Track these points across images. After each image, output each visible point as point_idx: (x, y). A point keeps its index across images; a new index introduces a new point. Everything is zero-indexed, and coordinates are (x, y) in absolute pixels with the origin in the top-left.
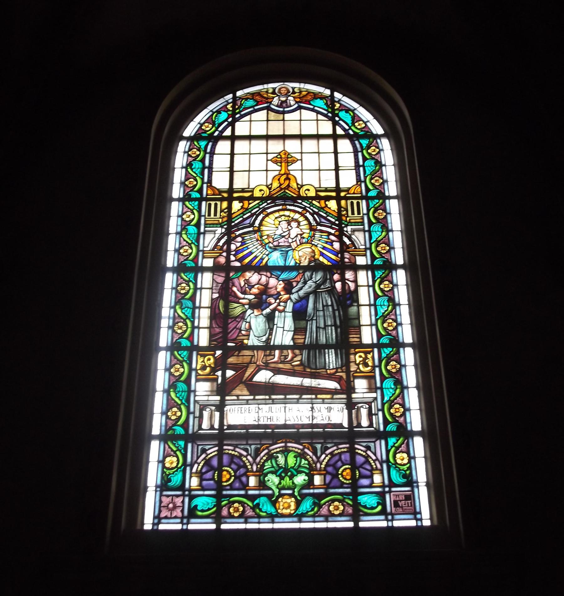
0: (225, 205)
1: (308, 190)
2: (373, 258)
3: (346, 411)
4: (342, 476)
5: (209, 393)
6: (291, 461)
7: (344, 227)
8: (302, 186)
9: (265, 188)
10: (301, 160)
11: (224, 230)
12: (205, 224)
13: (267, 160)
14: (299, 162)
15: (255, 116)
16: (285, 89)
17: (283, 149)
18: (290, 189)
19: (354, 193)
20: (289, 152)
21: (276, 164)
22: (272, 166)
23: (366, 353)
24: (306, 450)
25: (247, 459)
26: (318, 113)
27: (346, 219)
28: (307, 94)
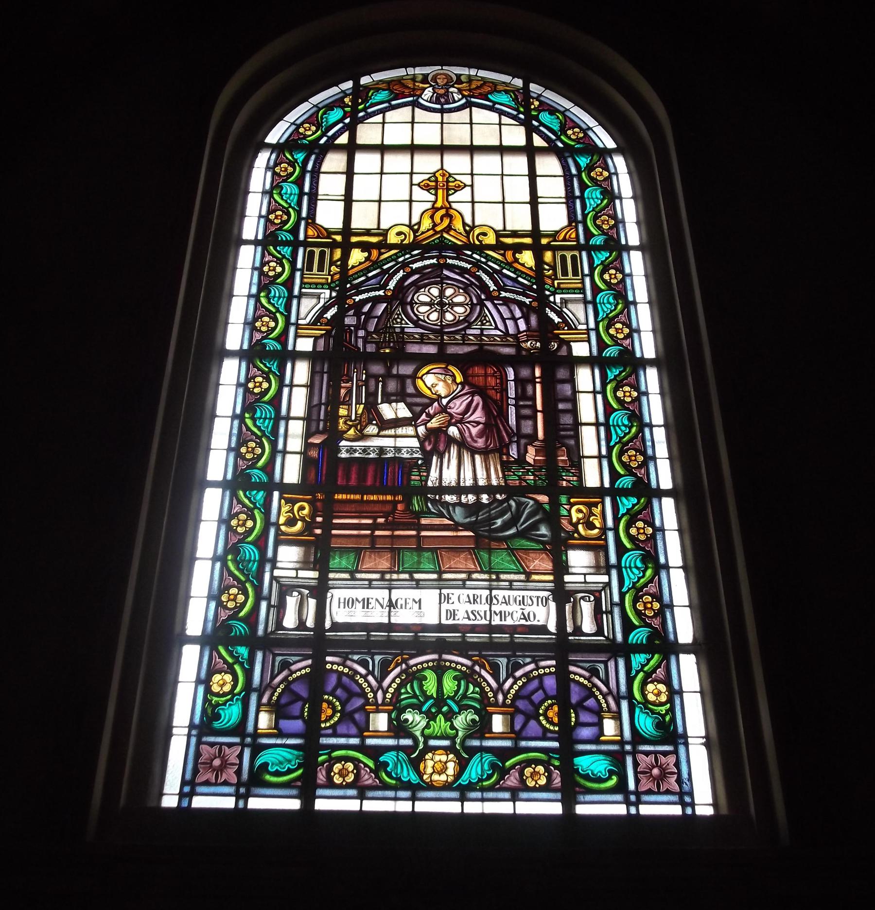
1: (485, 234)
2: (602, 345)
3: (553, 605)
5: (298, 566)
6: (449, 685)
7: (550, 295)
8: (473, 227)
9: (406, 230)
10: (472, 186)
11: (334, 294)
13: (412, 185)
14: (468, 189)
15: (390, 116)
16: (444, 77)
21: (428, 191)
22: (419, 194)
25: (366, 681)
26: (501, 113)
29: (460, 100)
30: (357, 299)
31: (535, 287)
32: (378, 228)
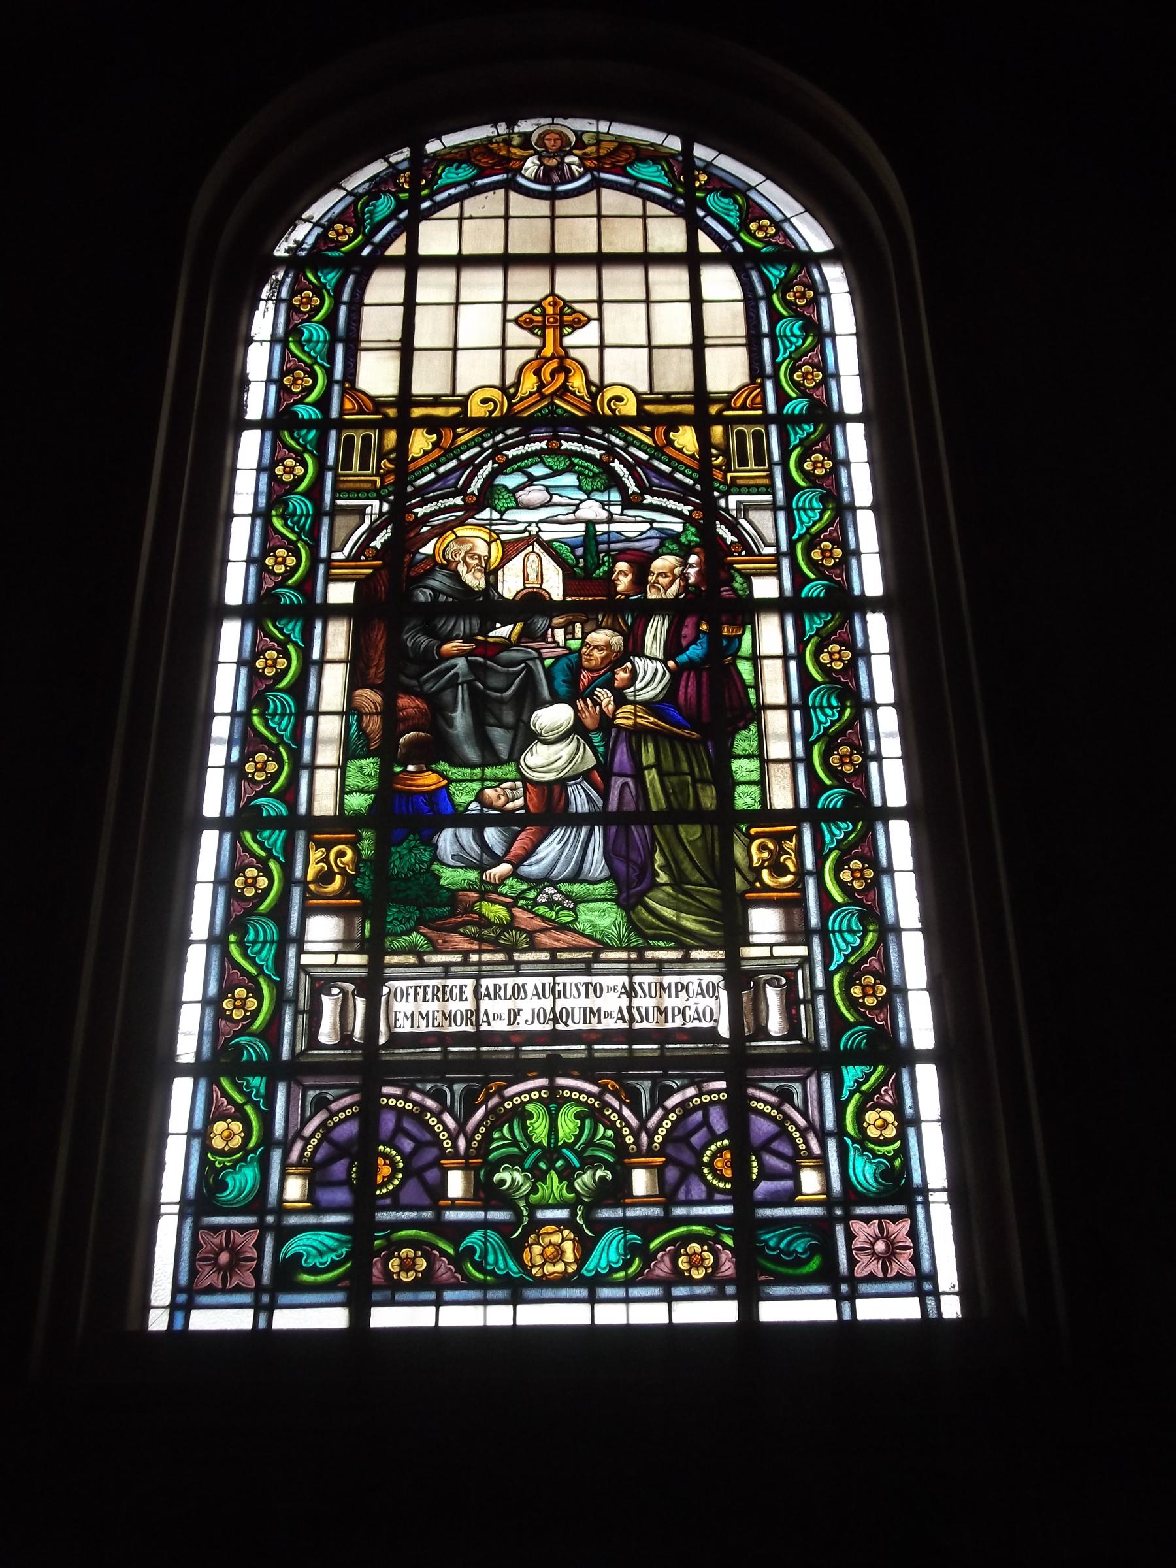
0: (391, 437)
1: (619, 399)
7: (720, 497)
8: (602, 387)
9: (496, 394)
10: (600, 319)
11: (386, 507)
12: (335, 489)
13: (505, 321)
14: (594, 325)
17: (548, 292)
19: (743, 407)
20: (567, 297)
21: (531, 331)
22: (517, 335)
26: (647, 197)
27: (725, 477)
28: (616, 149)
30: (420, 512)
32: (453, 394)
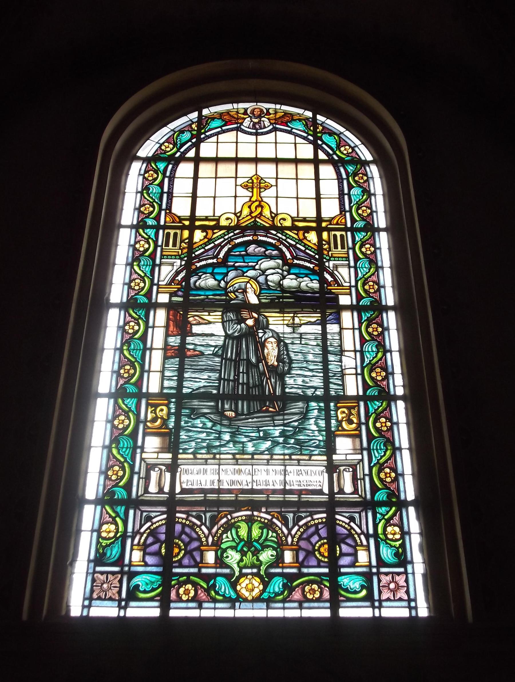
1: (284, 219)
4: (320, 553)
8: (277, 215)
9: (232, 216)
17: (255, 173)
18: (262, 218)
21: (247, 189)
22: (241, 191)
23: (349, 408)
24: (275, 520)
29: (268, 126)
31: (317, 256)
